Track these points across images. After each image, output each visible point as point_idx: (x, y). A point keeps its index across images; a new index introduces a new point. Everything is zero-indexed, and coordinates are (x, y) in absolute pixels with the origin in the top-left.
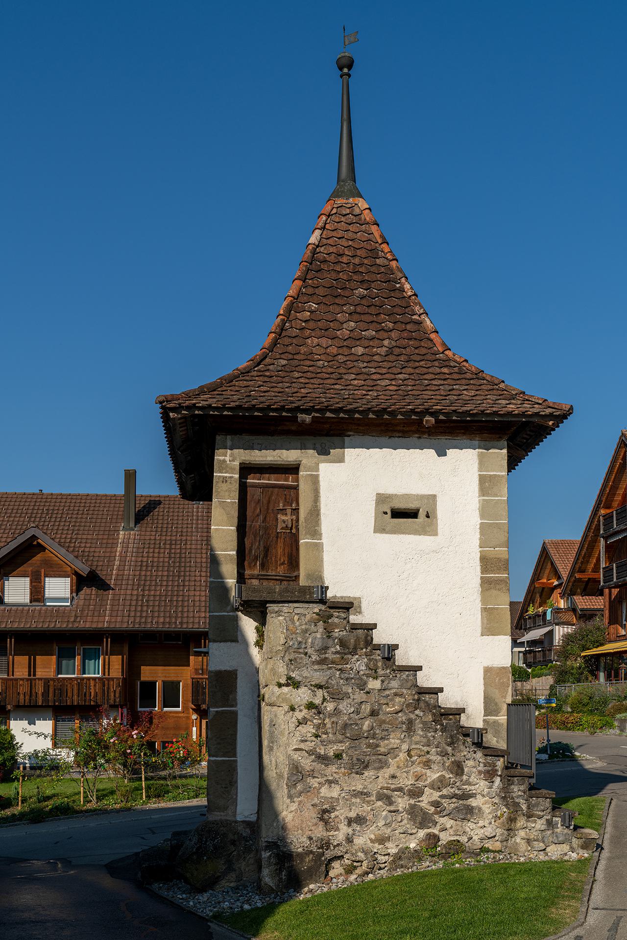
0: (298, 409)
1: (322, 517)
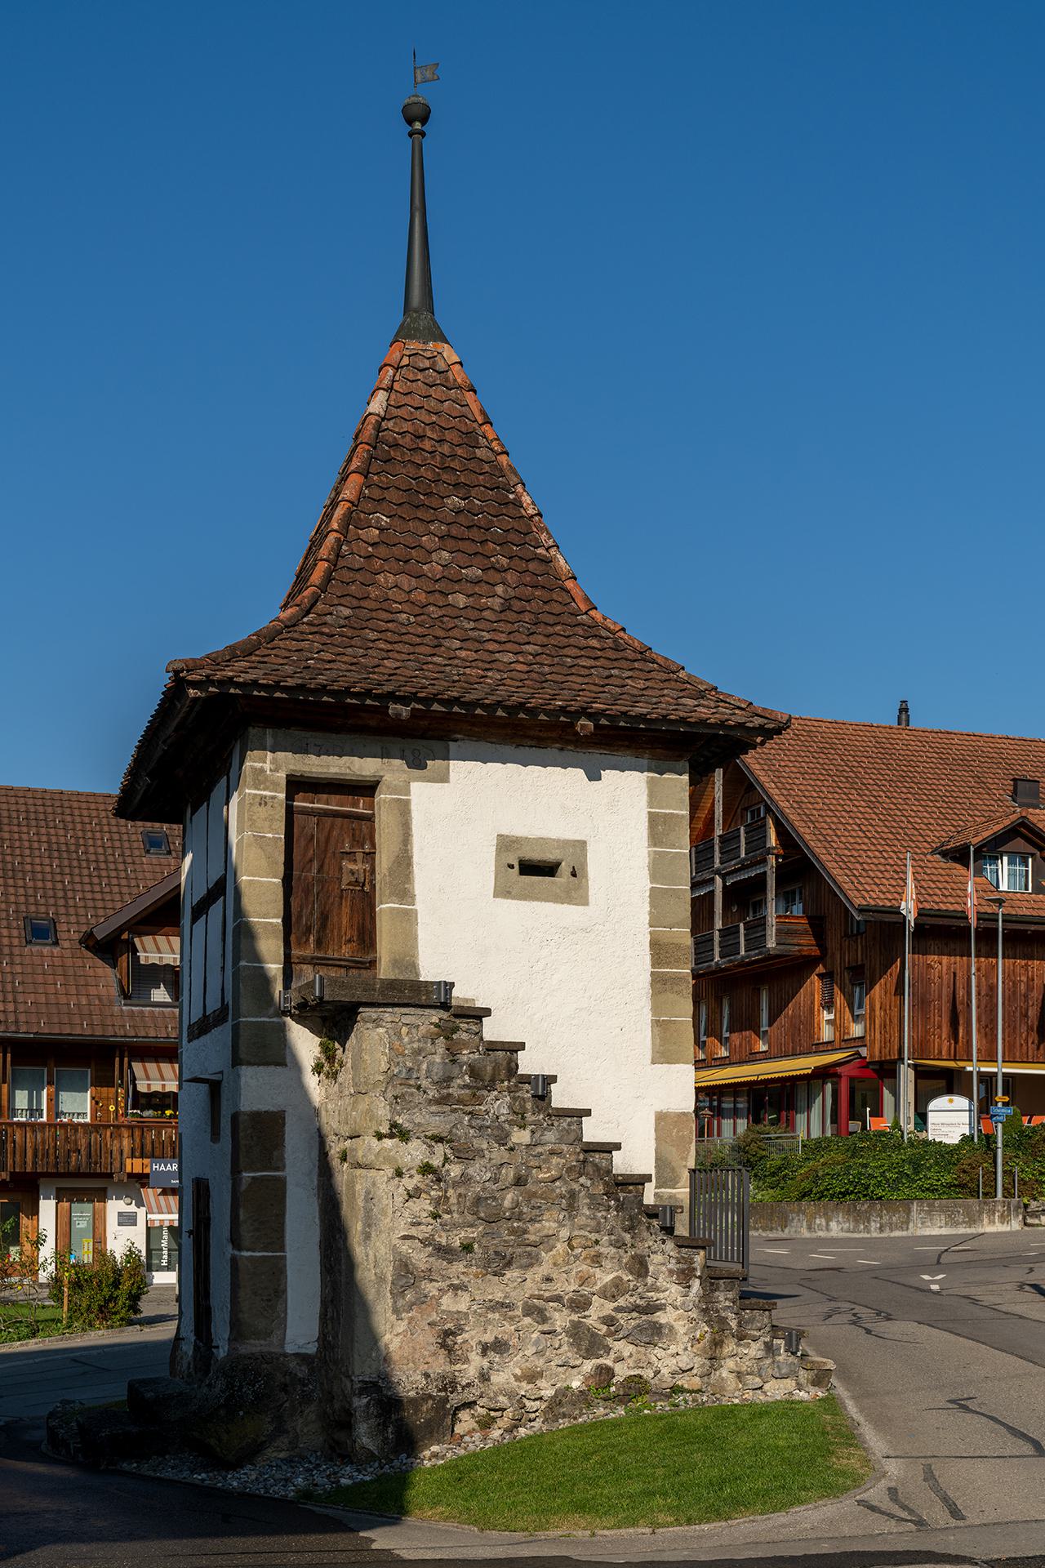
0: (391, 696)
1: (416, 869)
